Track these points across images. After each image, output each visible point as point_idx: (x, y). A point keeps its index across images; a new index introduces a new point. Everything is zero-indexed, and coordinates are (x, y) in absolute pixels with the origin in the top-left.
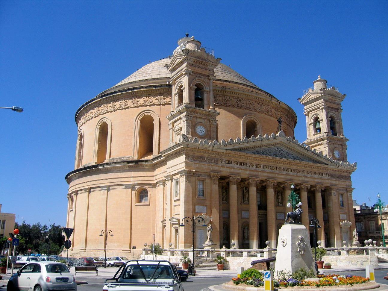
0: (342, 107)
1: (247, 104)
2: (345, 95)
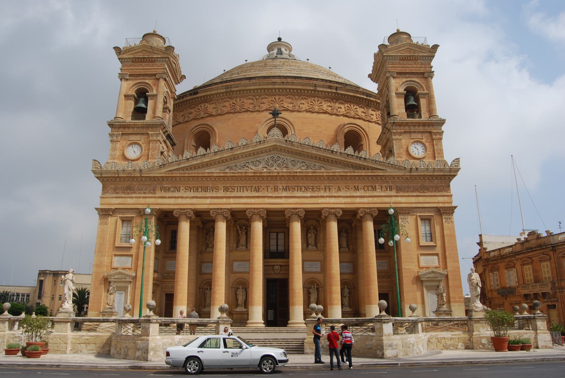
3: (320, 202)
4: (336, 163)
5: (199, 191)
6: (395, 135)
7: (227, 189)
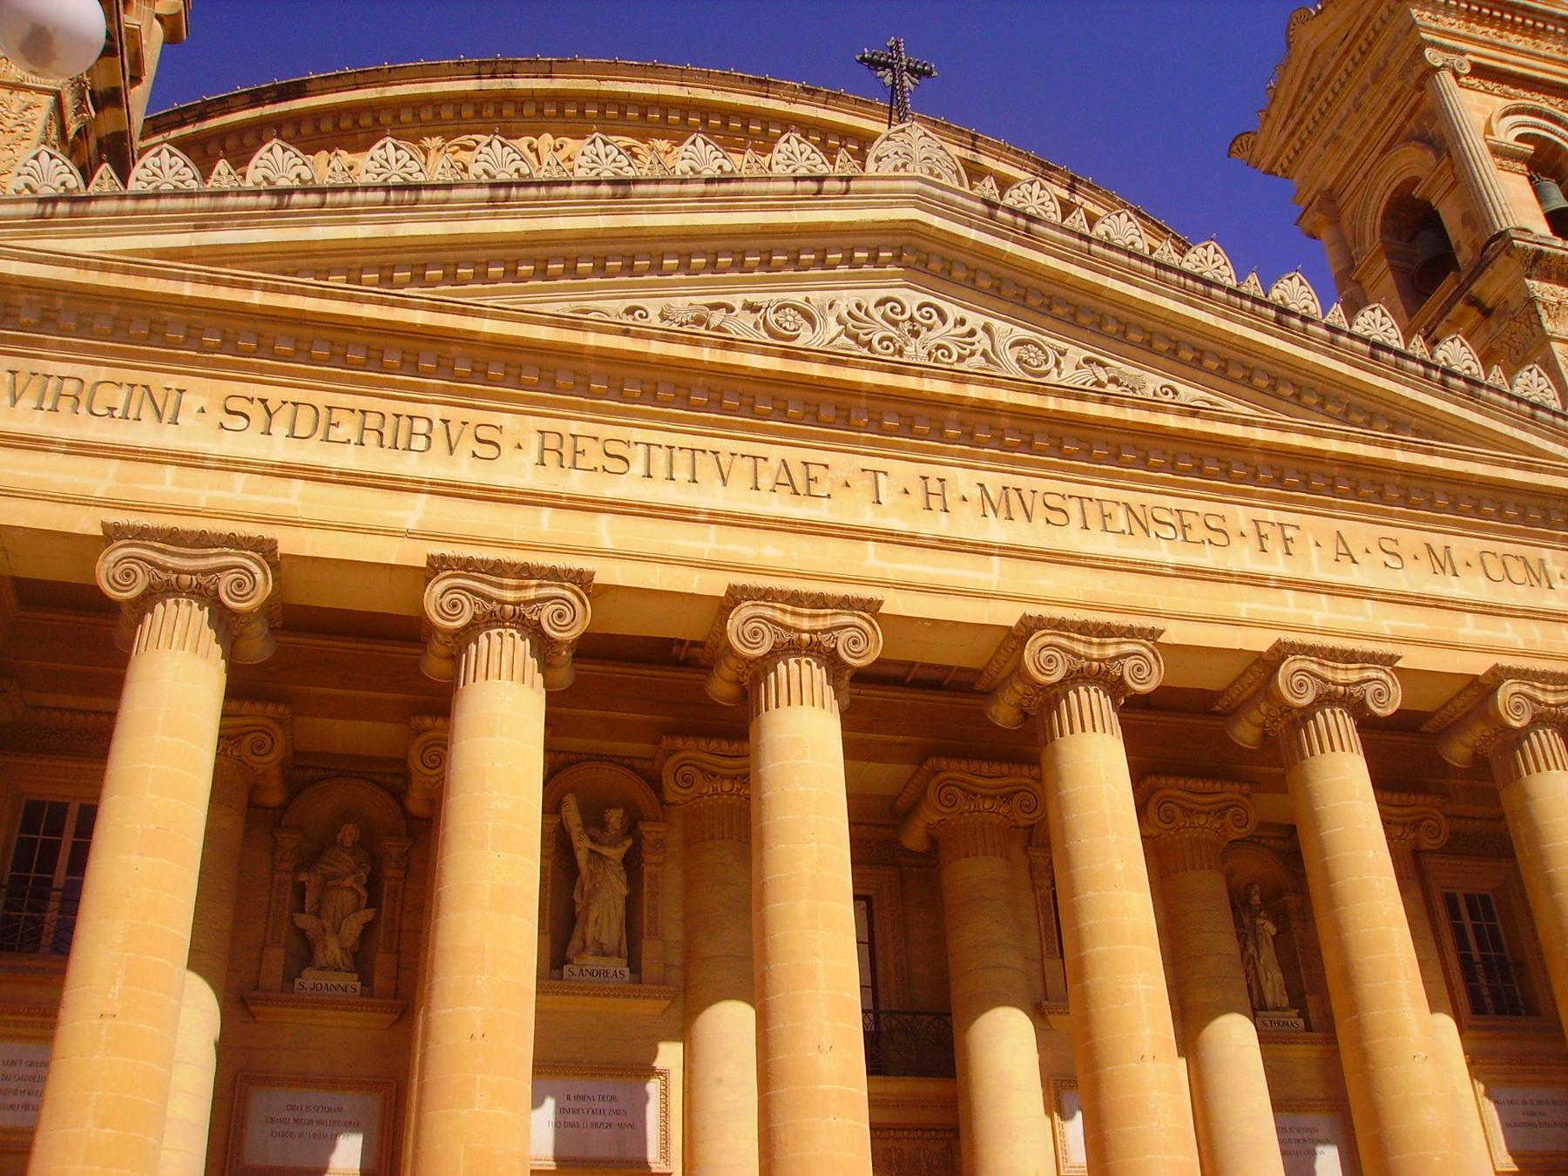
3: (1243, 615)
4: (1298, 396)
5: (336, 434)
7: (567, 452)
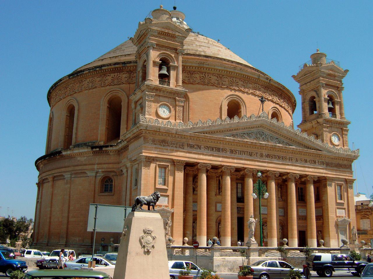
0: (343, 85)
1: (200, 77)
2: (347, 71)
6: (325, 128)
